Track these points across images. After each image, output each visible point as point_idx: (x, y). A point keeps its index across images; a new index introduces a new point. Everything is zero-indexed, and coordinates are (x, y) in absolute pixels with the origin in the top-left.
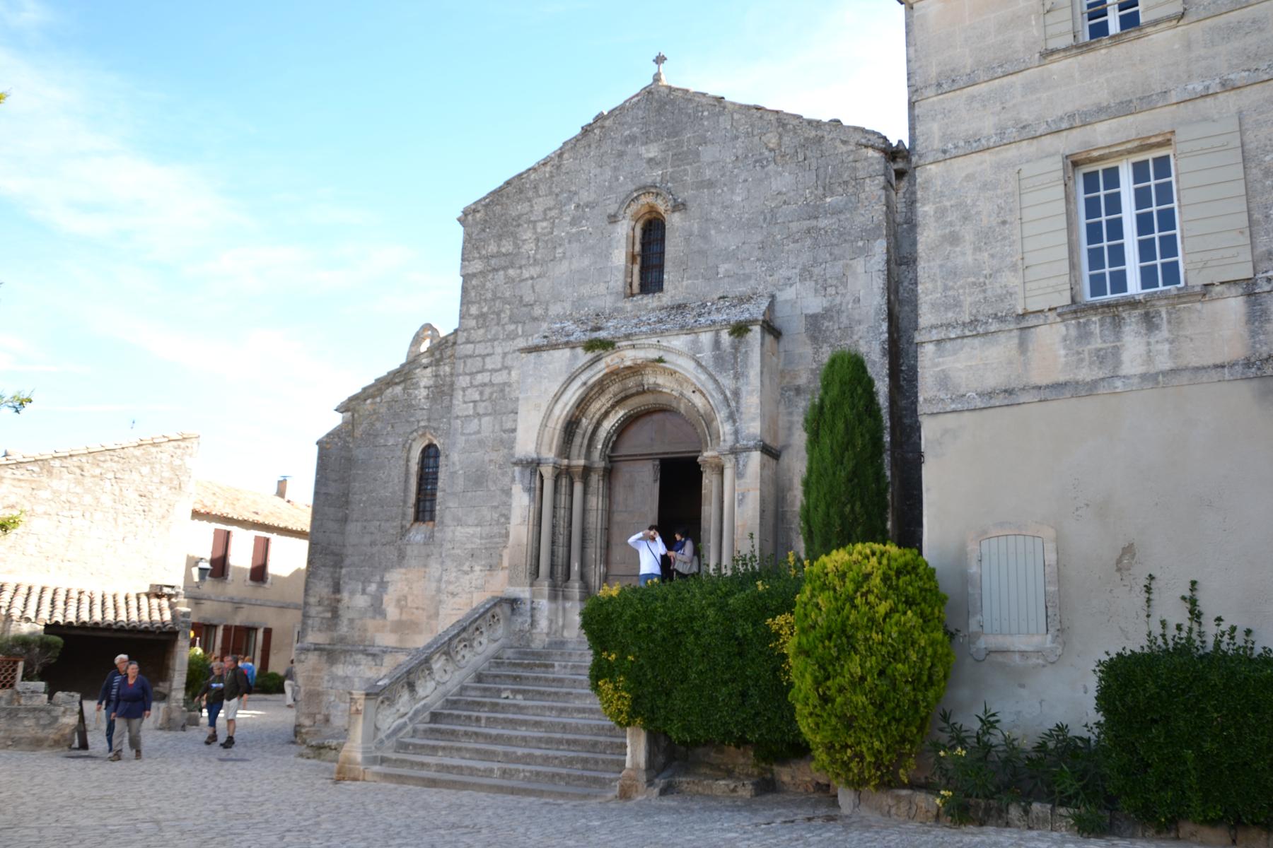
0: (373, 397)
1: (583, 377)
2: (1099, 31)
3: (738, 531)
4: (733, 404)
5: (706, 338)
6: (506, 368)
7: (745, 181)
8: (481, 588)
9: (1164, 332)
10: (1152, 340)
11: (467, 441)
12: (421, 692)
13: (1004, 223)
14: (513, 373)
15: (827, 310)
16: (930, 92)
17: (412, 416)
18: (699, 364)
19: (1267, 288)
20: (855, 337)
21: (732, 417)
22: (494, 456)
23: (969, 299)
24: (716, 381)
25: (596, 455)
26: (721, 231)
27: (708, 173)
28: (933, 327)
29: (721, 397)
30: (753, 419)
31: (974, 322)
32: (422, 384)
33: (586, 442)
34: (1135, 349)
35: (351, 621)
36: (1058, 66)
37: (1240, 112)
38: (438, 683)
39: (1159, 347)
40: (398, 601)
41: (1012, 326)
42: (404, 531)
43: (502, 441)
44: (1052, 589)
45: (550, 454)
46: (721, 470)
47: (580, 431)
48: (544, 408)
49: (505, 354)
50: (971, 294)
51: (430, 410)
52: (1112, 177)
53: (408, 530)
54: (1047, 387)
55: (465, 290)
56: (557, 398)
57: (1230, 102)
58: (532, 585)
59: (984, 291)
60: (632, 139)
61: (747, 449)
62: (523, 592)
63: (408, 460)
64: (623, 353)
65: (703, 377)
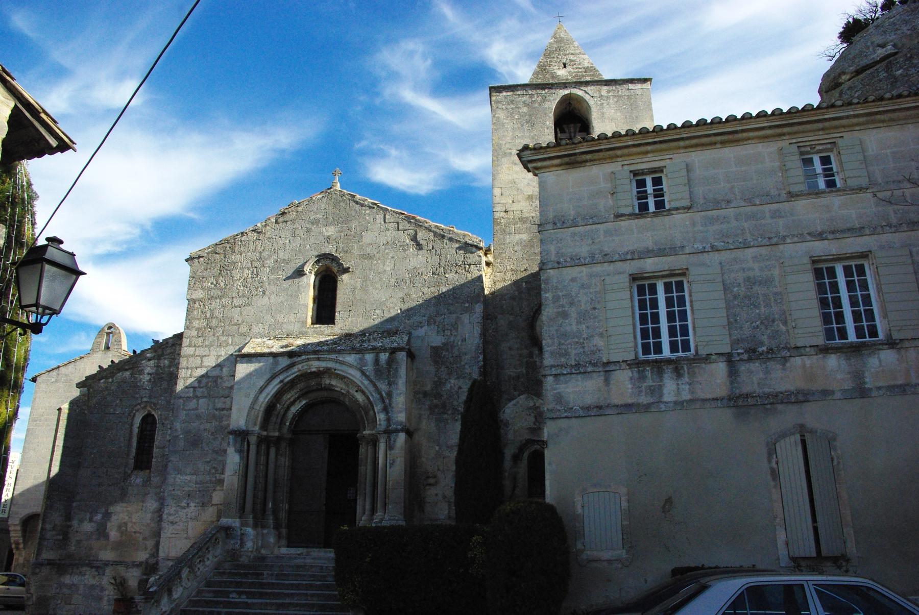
0: (106, 378)
1: (281, 377)
2: (644, 207)
3: (390, 484)
4: (387, 401)
5: (369, 357)
7: (393, 257)
8: (195, 519)
9: (686, 379)
10: (680, 382)
11: (187, 415)
12: (175, 595)
13: (595, 309)
14: (224, 370)
15: (445, 344)
16: (550, 226)
17: (137, 393)
18: (363, 373)
19: (738, 359)
21: (386, 410)
22: (208, 426)
23: (574, 352)
24: (375, 385)
25: (285, 430)
27: (368, 250)
28: (552, 366)
31: (578, 365)
32: (146, 372)
33: (279, 420)
34: (670, 388)
35: (79, 542)
36: (624, 224)
37: (721, 263)
38: (185, 588)
39: (684, 387)
40: (120, 527)
41: (600, 369)
42: (126, 477)
44: (626, 523)
45: (257, 428)
46: (374, 442)
47: (275, 413)
48: (252, 396)
50: (576, 349)
51: (151, 390)
52: (653, 289)
53: (130, 476)
54: (622, 406)
55: (189, 311)
56: (262, 390)
57: (716, 257)
58: (240, 518)
59: (583, 347)
60: (316, 222)
62: (236, 523)
63: (132, 425)
64: (310, 363)
65: (366, 382)
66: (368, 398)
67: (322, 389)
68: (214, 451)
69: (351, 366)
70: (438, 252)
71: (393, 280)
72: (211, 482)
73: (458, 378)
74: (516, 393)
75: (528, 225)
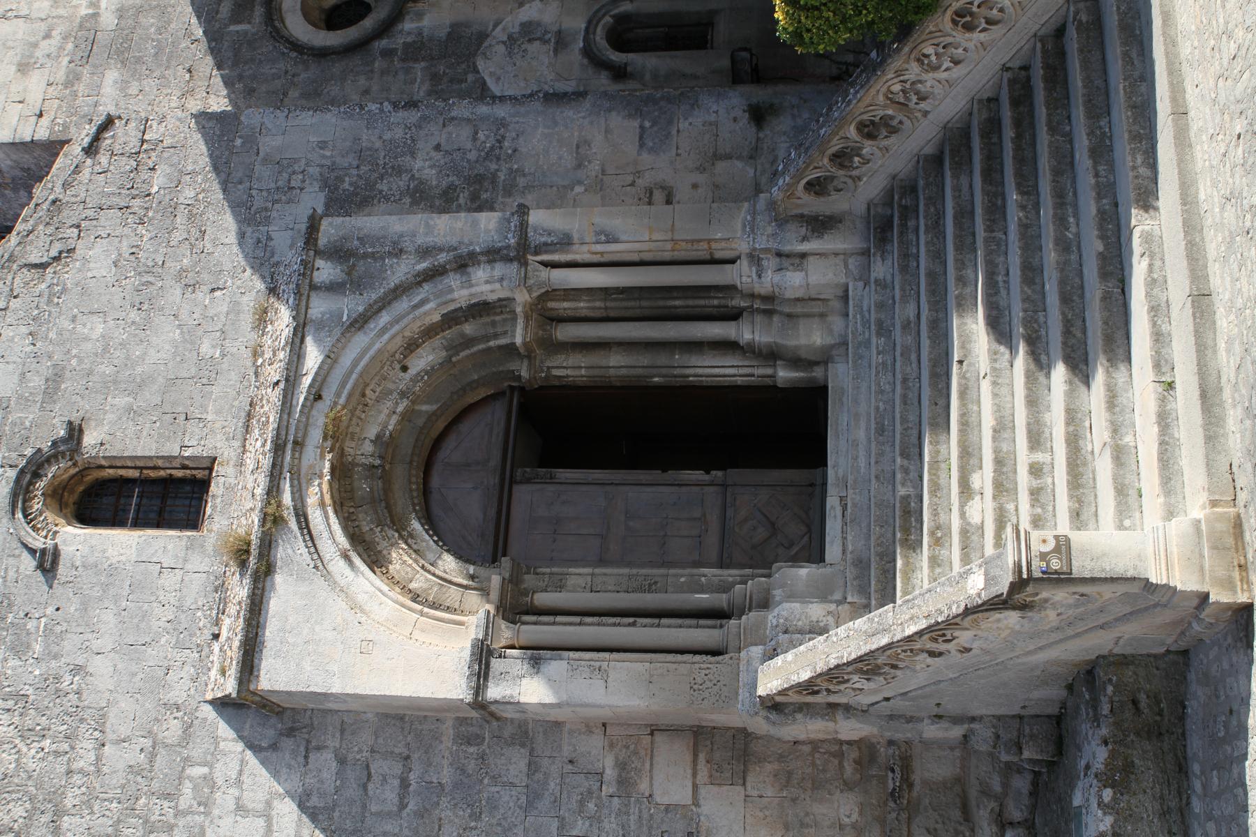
4: (442, 258)
6: (269, 804)
18: (360, 322)
20: (378, 144)
21: (463, 263)
26: (142, 358)
27: (36, 382)
29: (426, 286)
30: (475, 224)
43: (420, 814)
49: (241, 808)
61: (523, 226)
65: (384, 318)
66: (430, 332)
67: (386, 478)
68: (529, 807)
69: (330, 359)
70: (90, 213)
71: (134, 315)
72: (623, 812)
73: (413, 154)
74: (470, 77)
75: (86, 71)
